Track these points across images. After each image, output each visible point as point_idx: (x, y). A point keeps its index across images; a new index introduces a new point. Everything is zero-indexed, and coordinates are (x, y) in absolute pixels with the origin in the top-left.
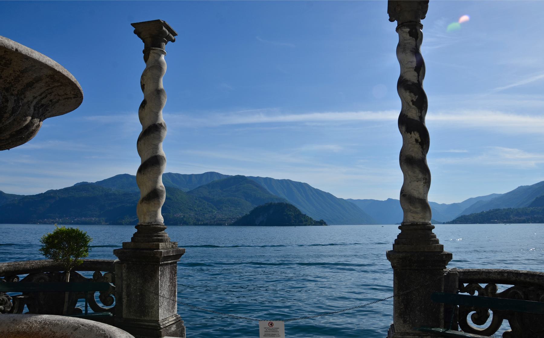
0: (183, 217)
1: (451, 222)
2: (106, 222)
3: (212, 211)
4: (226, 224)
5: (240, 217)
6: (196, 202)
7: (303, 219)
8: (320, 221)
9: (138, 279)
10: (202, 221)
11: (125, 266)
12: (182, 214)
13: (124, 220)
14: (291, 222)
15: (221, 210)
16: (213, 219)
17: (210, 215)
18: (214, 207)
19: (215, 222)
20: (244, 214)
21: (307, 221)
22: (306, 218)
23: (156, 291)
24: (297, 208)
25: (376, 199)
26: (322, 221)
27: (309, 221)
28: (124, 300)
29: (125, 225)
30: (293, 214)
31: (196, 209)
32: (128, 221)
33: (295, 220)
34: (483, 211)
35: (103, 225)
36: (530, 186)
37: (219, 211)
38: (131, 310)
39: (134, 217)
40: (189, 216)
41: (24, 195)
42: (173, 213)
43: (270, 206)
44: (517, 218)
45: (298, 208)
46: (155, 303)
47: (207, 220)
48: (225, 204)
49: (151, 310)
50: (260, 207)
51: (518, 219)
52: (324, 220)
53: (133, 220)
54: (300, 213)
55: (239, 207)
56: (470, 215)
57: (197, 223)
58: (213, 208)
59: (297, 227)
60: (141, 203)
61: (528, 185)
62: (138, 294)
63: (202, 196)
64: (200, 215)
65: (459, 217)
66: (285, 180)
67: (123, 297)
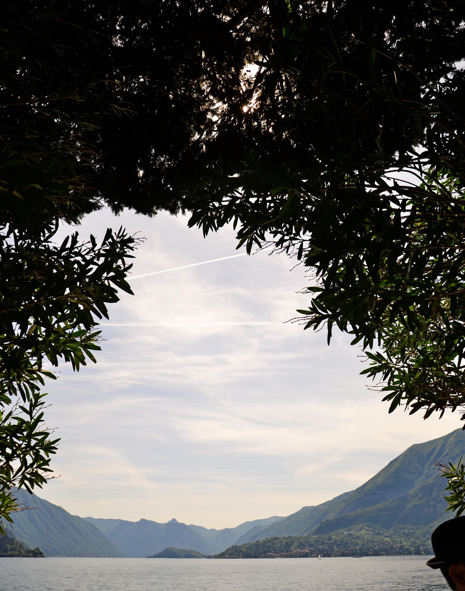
25: (124, 520)
34: (259, 540)
36: (316, 506)
44: (299, 551)
51: (299, 552)
56: (243, 545)
61: (313, 505)
65: (229, 548)
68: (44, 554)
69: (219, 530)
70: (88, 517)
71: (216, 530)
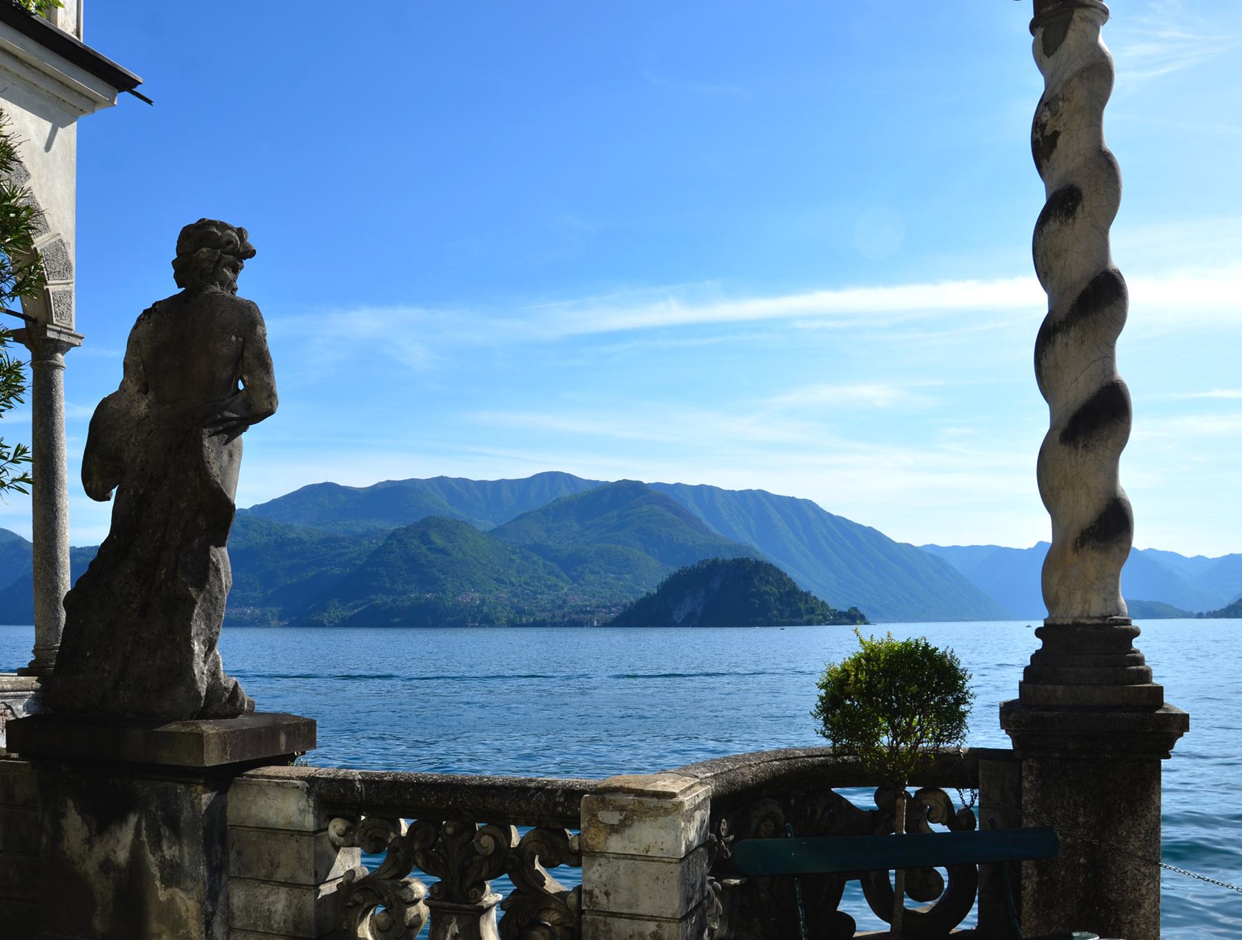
0: (479, 604)
1: (1221, 610)
2: (281, 618)
4: (595, 622)
5: (631, 603)
6: (513, 561)
7: (802, 606)
8: (849, 611)
9: (1082, 811)
10: (531, 614)
11: (1031, 768)
12: (477, 595)
13: (326, 614)
14: (769, 614)
15: (581, 582)
16: (560, 607)
17: (550, 598)
18: (563, 574)
19: (564, 616)
20: (642, 592)
21: (812, 611)
22: (812, 602)
23: (1148, 852)
24: (785, 574)
25: (1003, 546)
26: (855, 613)
27: (818, 612)
28: (1026, 883)
29: (330, 627)
30: (776, 591)
31: (513, 579)
32: (338, 616)
33: (781, 608)
35: (274, 627)
38: (1055, 918)
39: (351, 604)
40: (496, 601)
41: (75, 545)
42: (453, 593)
43: (712, 570)
45: (789, 575)
46: (1144, 891)
47: (541, 611)
49: (1130, 917)
50: (684, 571)
52: (858, 609)
53: (349, 614)
54: (795, 587)
55: (628, 573)
57: (518, 620)
58: (557, 577)
59: (787, 629)
60: (1076, 549)
62: (1082, 860)
63: (528, 543)
64: (526, 597)
67: (1024, 872)
68: (868, 619)
69: (1213, 559)
70: (928, 543)
71: (1207, 558)
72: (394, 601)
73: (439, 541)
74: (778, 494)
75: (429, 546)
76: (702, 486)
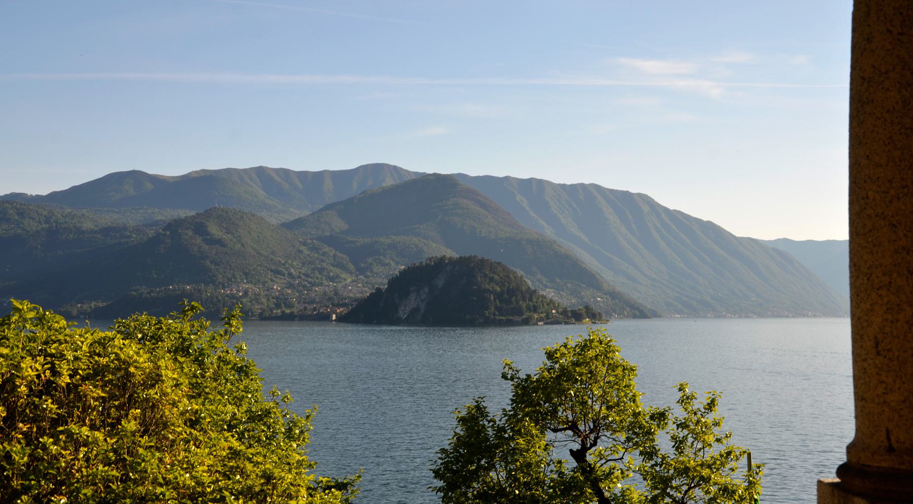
3: (338, 277)
6: (301, 252)
37: (362, 277)
48: (382, 257)
66: (582, 185)
72: (149, 293)
73: (214, 230)
74: (612, 188)
75: (205, 237)
76: (532, 179)
